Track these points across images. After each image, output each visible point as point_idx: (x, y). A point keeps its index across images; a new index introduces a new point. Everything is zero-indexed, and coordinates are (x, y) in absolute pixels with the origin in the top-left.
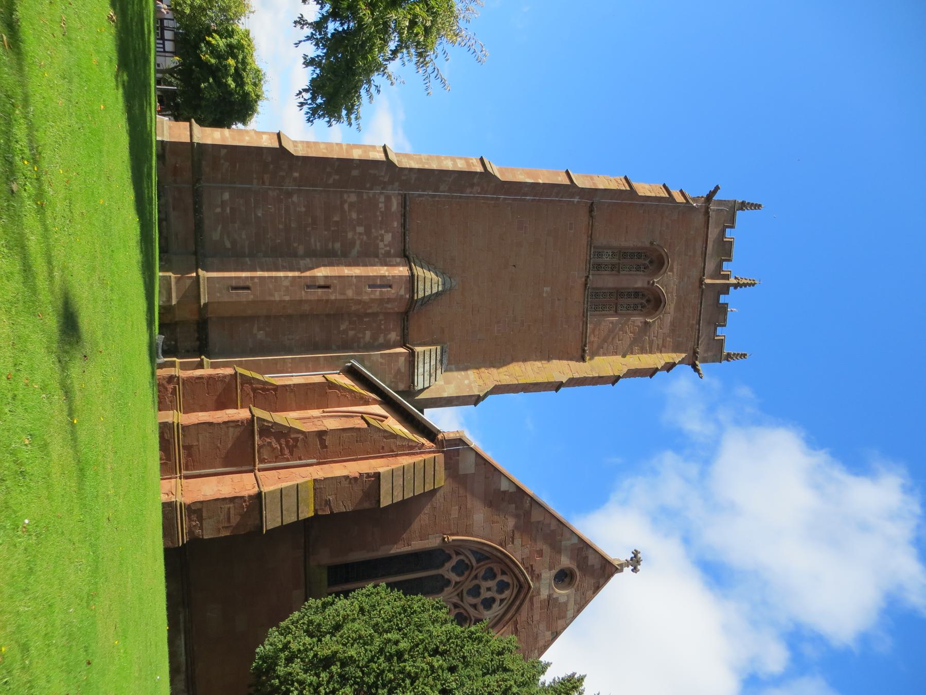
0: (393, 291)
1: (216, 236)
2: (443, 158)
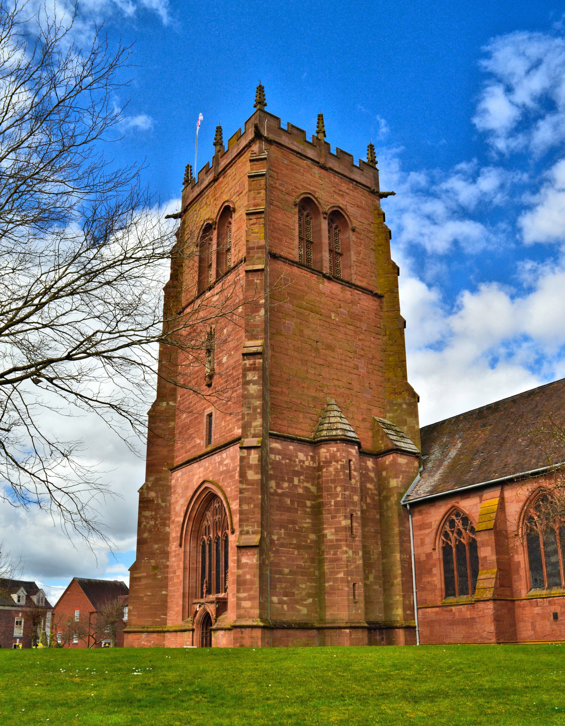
0: (354, 460)
1: (304, 611)
2: (246, 392)
